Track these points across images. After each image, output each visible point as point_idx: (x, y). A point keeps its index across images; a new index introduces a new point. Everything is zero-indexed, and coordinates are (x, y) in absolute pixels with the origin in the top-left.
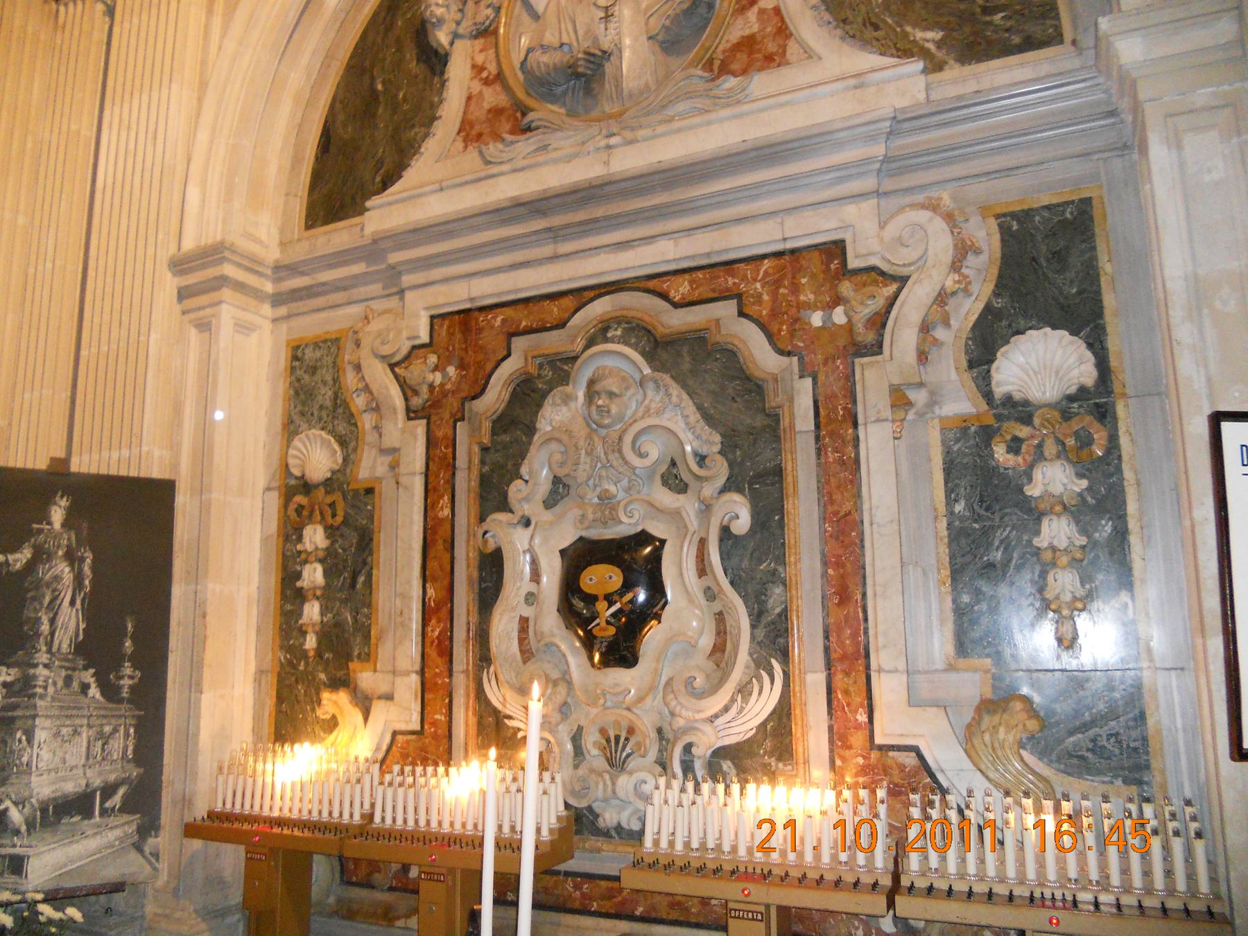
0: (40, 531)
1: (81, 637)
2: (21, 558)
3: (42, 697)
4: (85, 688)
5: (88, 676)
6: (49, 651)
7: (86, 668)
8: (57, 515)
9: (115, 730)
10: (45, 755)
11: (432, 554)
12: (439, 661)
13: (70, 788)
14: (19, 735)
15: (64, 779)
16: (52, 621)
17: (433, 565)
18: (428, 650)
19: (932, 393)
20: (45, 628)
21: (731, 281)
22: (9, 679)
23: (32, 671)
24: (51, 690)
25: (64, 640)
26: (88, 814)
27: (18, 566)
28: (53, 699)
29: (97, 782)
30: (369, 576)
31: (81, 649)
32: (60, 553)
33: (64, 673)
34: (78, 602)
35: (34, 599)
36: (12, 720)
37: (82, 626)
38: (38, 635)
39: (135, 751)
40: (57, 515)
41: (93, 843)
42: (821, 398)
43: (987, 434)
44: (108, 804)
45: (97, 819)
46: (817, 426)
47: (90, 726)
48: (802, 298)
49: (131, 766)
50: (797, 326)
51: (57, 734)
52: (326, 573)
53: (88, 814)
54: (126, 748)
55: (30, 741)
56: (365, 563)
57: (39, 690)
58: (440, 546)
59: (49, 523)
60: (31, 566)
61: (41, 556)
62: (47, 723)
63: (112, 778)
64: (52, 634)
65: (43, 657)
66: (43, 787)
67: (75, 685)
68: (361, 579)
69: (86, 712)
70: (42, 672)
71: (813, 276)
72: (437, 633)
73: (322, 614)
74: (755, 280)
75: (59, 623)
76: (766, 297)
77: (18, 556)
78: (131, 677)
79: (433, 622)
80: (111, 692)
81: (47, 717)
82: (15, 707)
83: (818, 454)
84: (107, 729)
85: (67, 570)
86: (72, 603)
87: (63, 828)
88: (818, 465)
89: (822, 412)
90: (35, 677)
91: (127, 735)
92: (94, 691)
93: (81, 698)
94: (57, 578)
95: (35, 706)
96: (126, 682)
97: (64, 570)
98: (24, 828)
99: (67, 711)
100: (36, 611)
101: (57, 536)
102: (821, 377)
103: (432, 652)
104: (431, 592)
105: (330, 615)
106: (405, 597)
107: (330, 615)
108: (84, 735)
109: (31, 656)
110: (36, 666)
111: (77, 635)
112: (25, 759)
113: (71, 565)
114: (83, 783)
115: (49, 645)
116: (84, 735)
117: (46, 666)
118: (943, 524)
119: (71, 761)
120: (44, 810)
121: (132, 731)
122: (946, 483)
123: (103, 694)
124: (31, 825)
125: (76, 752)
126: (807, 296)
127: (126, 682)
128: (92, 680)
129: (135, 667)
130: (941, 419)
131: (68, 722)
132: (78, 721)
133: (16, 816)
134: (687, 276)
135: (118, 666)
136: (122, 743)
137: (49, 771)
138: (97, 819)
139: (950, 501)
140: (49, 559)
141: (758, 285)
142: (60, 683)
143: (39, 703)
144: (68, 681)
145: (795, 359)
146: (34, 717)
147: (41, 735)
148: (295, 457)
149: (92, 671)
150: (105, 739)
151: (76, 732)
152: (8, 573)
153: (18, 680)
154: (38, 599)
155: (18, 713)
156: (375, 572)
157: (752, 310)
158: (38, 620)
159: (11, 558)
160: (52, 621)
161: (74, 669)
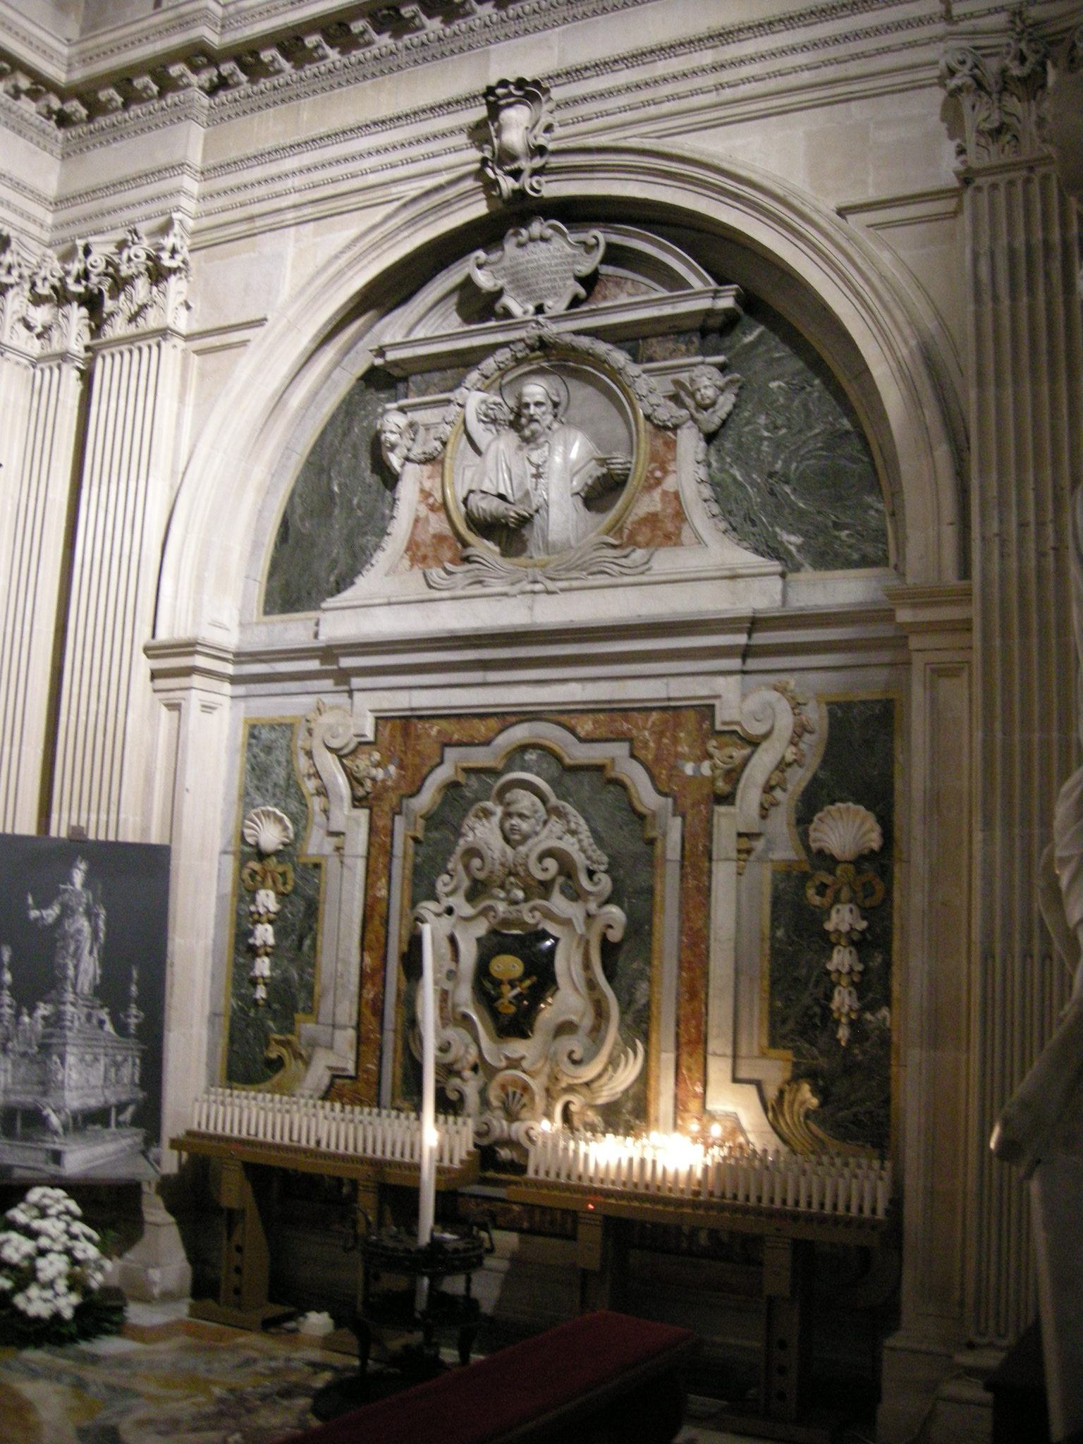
0: (65, 891)
1: (98, 981)
2: (51, 913)
3: (70, 1029)
4: (101, 1023)
5: (104, 1014)
6: (75, 993)
7: (102, 1007)
8: (78, 877)
9: (125, 1060)
10: (74, 1075)
11: (370, 927)
12: (372, 1019)
13: (93, 1103)
14: (55, 1058)
15: (88, 1096)
16: (76, 967)
17: (370, 936)
18: (364, 1010)
19: (768, 841)
20: (71, 972)
21: (626, 726)
22: (46, 1013)
23: (62, 1008)
24: (76, 1023)
25: (85, 984)
26: (106, 1124)
27: (50, 920)
28: (79, 1031)
29: (113, 1100)
30: (314, 940)
31: (98, 991)
32: (81, 909)
33: (85, 1010)
34: (95, 952)
35: (62, 948)
36: (50, 1045)
37: (99, 971)
38: (66, 978)
39: (141, 1079)
40: (78, 877)
41: (110, 1147)
42: (687, 835)
43: (805, 877)
44: (122, 1118)
45: (113, 1128)
46: (683, 857)
47: (106, 1055)
48: (680, 749)
49: (137, 1089)
50: (674, 773)
51: (82, 1060)
52: (277, 934)
53: (106, 1124)
54: (133, 1075)
55: (63, 1063)
56: (311, 928)
57: (68, 1024)
58: (377, 921)
59: (73, 884)
60: (59, 920)
61: (67, 912)
62: (74, 1050)
63: (124, 1097)
64: (76, 977)
65: (70, 997)
66: (74, 1100)
67: (95, 1021)
68: (307, 942)
69: (103, 1044)
70: (69, 1009)
71: (689, 733)
72: (371, 995)
73: (272, 970)
74: (644, 728)
75: (82, 967)
76: (652, 744)
77: (50, 912)
78: (136, 1017)
79: (369, 986)
80: (121, 1028)
81: (74, 1045)
82: (51, 1035)
83: (681, 880)
84: (119, 1058)
85: (86, 924)
86: (91, 952)
87: (88, 1133)
88: (682, 889)
89: (687, 847)
90: (63, 1013)
91: (134, 1064)
92: (109, 1027)
93: (99, 1031)
94: (79, 931)
95: (65, 1036)
96: (133, 1021)
97: (84, 924)
98: (61, 1130)
99: (89, 1042)
100: (64, 958)
101: (78, 895)
102: (689, 818)
103: (367, 1012)
104: (368, 959)
105: (279, 971)
106: (346, 963)
107: (279, 971)
108: (102, 1062)
109: (61, 994)
110: (64, 1003)
111: (95, 978)
112: (60, 1077)
113: (90, 921)
114: (102, 1099)
115: (74, 986)
116: (102, 1062)
117: (73, 1004)
118: (767, 945)
119: (93, 1081)
120: (75, 1119)
121: (138, 1061)
122: (773, 912)
123: (116, 1031)
124: (65, 1127)
125: (97, 1075)
126: (683, 749)
127: (133, 1021)
128: (106, 1018)
129: (139, 1007)
130: (772, 861)
131: (89, 1050)
132: (97, 1050)
133: (55, 1120)
134: (591, 716)
135: (126, 1008)
136: (130, 1071)
137: (77, 1088)
138: (113, 1128)
139: (774, 928)
140: (72, 916)
141: (646, 733)
142: (83, 1018)
143: (68, 1034)
144: (89, 1017)
145: (670, 800)
146: (65, 1044)
147: (71, 1059)
148: (251, 835)
149: (106, 1010)
150: (118, 1066)
151: (96, 1060)
152: (44, 926)
153: (53, 1014)
154: (65, 948)
155: (54, 1041)
156: (319, 937)
157: (641, 753)
158: (65, 967)
159: (45, 913)
160: (76, 967)
161: (92, 1008)
